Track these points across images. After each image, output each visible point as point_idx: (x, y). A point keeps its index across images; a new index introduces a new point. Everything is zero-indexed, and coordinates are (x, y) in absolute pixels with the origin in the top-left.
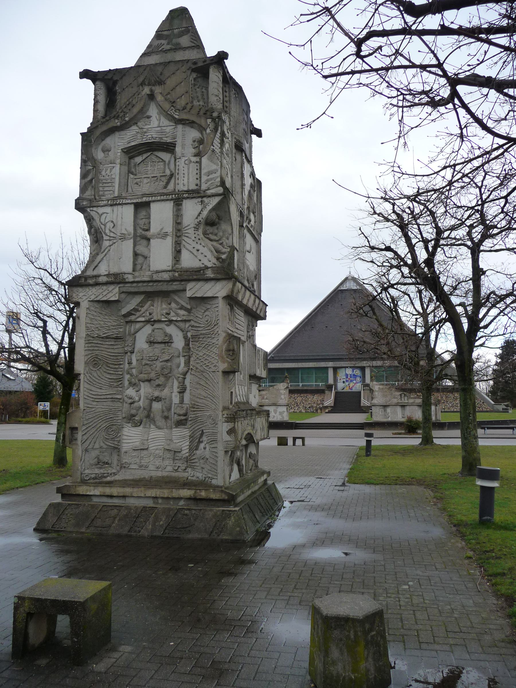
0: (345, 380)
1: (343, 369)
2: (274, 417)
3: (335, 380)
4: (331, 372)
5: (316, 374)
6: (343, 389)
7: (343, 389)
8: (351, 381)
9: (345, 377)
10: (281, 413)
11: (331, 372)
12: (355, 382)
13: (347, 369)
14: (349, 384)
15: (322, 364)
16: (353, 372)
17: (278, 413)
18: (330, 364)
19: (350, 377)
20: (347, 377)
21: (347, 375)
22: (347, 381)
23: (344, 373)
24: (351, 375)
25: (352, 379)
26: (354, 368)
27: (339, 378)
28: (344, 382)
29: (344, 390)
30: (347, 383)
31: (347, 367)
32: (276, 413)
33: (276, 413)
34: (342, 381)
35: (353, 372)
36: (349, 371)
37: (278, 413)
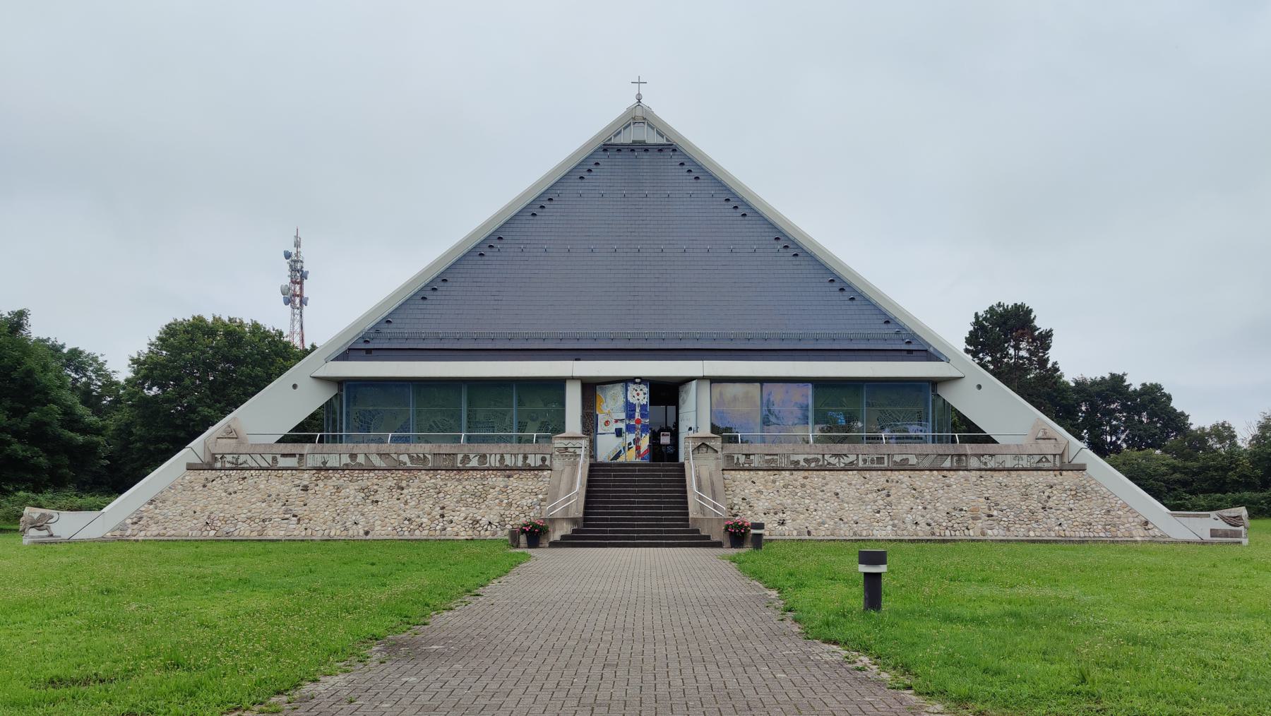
0: (622, 426)
1: (619, 389)
3: (590, 423)
4: (573, 397)
5: (520, 403)
6: (618, 456)
7: (618, 456)
9: (623, 416)
11: (573, 397)
13: (631, 387)
14: (636, 441)
19: (643, 416)
20: (630, 416)
21: (630, 408)
22: (630, 429)
23: (621, 402)
27: (601, 419)
28: (619, 433)
29: (621, 459)
30: (630, 437)
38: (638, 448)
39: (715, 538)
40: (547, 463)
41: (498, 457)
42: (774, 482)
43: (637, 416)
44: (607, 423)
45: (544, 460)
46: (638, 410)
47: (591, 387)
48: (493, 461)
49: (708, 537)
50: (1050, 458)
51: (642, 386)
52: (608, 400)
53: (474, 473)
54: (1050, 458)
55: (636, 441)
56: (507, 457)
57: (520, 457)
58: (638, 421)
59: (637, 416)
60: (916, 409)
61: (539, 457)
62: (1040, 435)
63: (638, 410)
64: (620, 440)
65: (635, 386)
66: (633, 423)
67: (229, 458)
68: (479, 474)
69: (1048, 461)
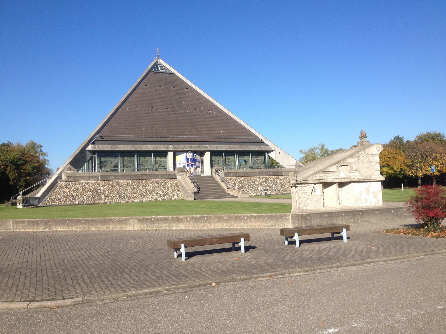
2: (366, 200)
8: (192, 166)
9: (186, 162)
10: (375, 194)
12: (195, 166)
13: (187, 153)
14: (190, 169)
15: (162, 147)
16: (193, 156)
18: (171, 147)
19: (191, 162)
20: (188, 162)
21: (188, 159)
22: (188, 165)
24: (191, 159)
25: (192, 163)
26: (194, 152)
31: (188, 151)
32: (368, 194)
33: (368, 194)
35: (193, 156)
36: (190, 155)
38: (190, 171)
39: (235, 196)
42: (238, 180)
43: (190, 162)
55: (190, 169)
58: (190, 163)
59: (190, 162)
66: (188, 164)
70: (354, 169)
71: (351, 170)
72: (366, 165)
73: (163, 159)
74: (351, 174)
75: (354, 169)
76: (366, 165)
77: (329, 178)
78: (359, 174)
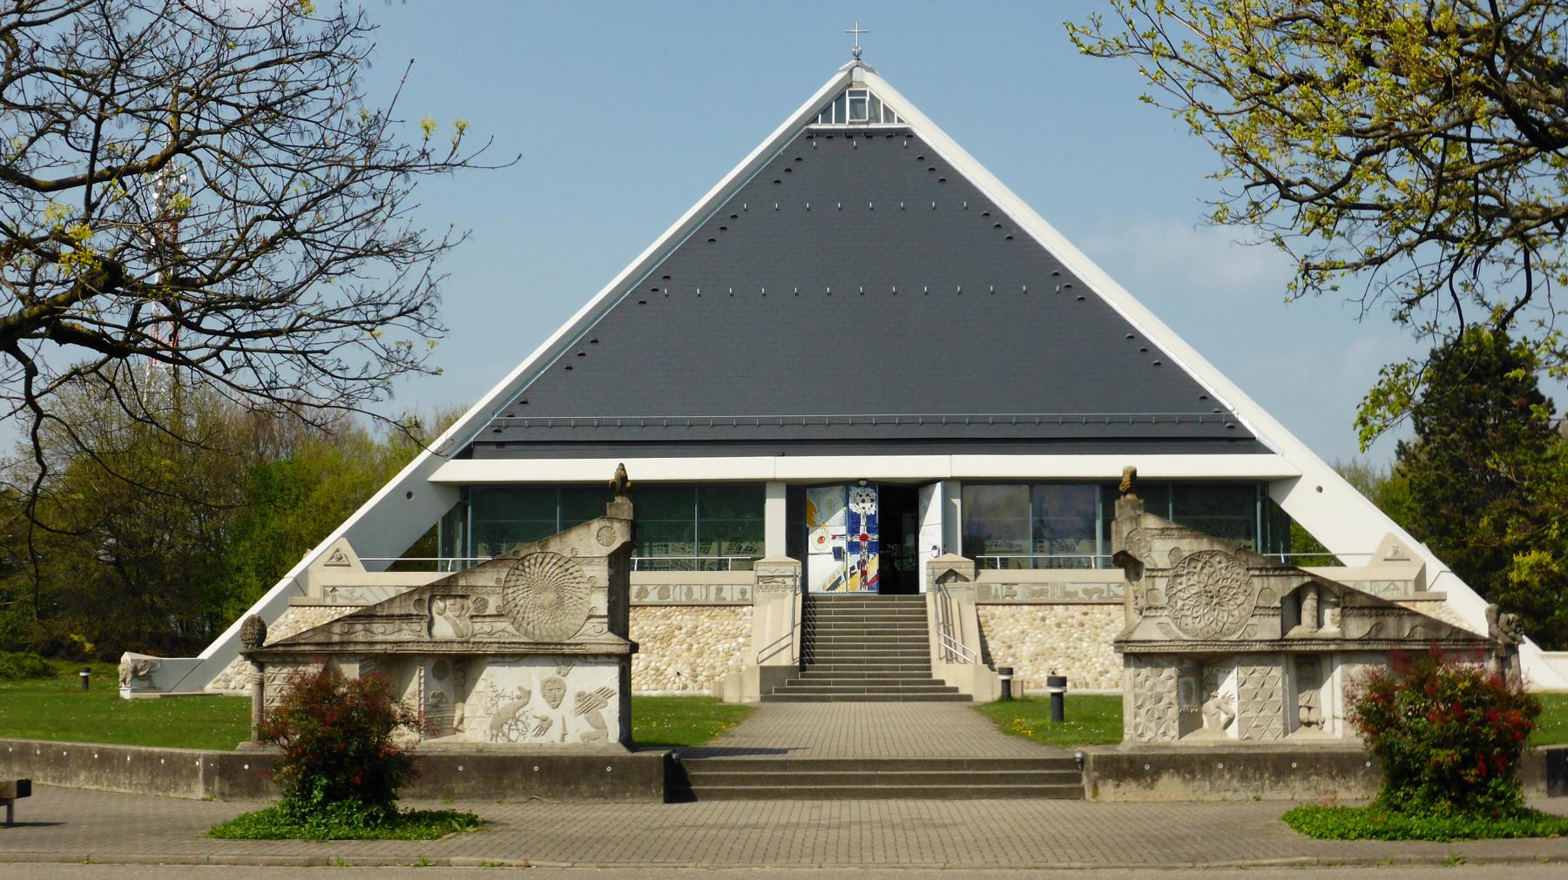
0: (842, 544)
1: (837, 494)
2: (544, 725)
6: (835, 585)
7: (835, 585)
9: (843, 530)
10: (587, 704)
14: (862, 564)
17: (569, 702)
19: (869, 530)
21: (853, 521)
22: (853, 547)
23: (841, 514)
28: (838, 554)
29: (841, 589)
30: (853, 559)
32: (555, 702)
33: (555, 702)
34: (830, 545)
37: (569, 702)
38: (864, 573)
40: (748, 596)
41: (684, 589)
42: (1043, 619)
44: (821, 540)
45: (743, 592)
46: (863, 522)
47: (800, 495)
48: (678, 596)
49: (956, 689)
50: (1401, 585)
51: (869, 490)
52: (823, 509)
53: (653, 610)
54: (1401, 585)
56: (696, 589)
57: (713, 590)
58: (864, 538)
59: (863, 530)
60: (1242, 518)
61: (737, 589)
62: (1389, 555)
63: (863, 522)
64: (840, 563)
65: (859, 490)
66: (856, 539)
67: (341, 591)
68: (660, 612)
69: (1397, 588)
70: (491, 610)
71: (478, 616)
72: (549, 597)
73: (748, 518)
74: (477, 626)
75: (491, 610)
76: (549, 597)
77: (380, 638)
78: (510, 629)
